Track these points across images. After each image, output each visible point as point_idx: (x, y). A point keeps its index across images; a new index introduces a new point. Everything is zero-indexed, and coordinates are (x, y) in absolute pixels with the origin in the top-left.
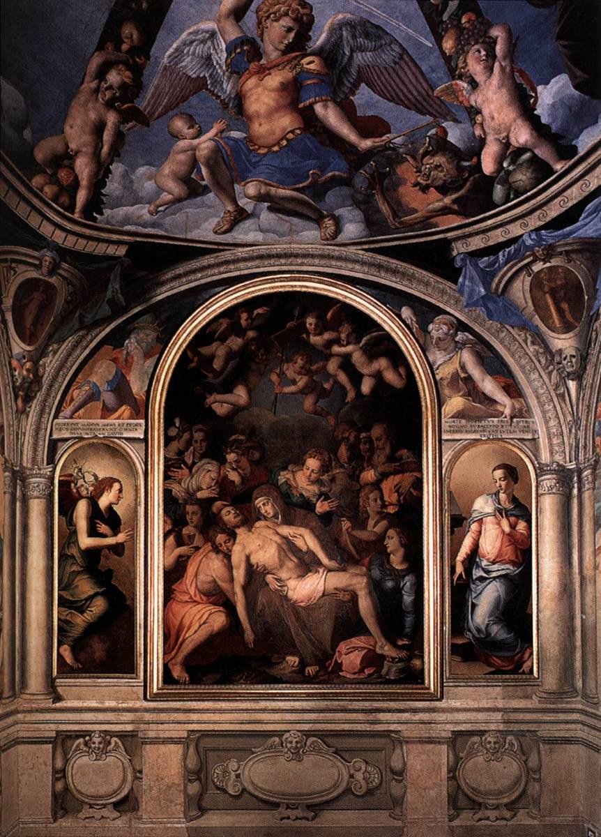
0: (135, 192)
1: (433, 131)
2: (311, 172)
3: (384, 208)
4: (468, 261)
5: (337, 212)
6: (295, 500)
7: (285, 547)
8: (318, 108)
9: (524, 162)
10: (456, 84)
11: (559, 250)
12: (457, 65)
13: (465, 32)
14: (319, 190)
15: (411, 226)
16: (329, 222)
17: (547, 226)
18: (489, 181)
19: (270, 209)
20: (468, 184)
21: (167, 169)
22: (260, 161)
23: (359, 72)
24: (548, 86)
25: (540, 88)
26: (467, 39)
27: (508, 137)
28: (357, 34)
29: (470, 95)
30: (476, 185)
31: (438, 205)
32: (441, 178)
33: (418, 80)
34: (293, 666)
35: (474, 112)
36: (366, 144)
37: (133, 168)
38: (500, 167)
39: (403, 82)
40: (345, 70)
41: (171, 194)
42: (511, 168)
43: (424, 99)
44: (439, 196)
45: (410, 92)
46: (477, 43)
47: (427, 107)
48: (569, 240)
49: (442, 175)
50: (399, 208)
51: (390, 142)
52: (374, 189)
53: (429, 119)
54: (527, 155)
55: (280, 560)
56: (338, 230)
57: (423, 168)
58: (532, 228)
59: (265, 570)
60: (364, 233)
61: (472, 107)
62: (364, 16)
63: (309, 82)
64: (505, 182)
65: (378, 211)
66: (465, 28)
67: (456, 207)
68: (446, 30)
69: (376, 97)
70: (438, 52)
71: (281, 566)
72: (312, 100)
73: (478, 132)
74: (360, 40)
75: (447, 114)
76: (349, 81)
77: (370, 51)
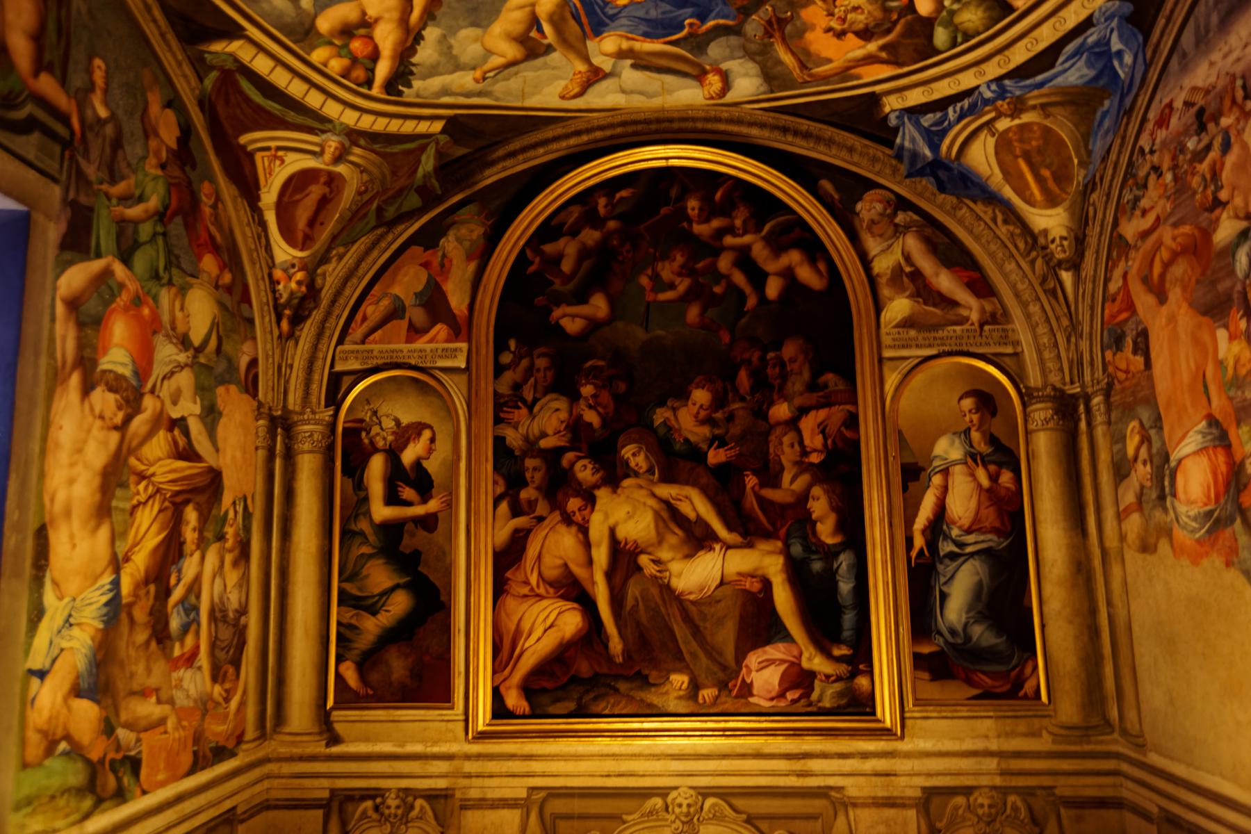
0: (455, 58)
2: (687, 22)
3: (787, 58)
4: (906, 120)
5: (725, 66)
6: (677, 447)
7: (665, 515)
11: (1032, 102)
14: (699, 43)
15: (825, 79)
16: (714, 81)
17: (1009, 75)
18: (928, 24)
19: (634, 66)
20: (899, 28)
21: (498, 28)
22: (620, 12)
30: (909, 32)
31: (859, 53)
32: (861, 22)
34: (680, 689)
37: (453, 31)
41: (502, 56)
42: (955, 7)
44: (860, 42)
48: (1045, 90)
49: (861, 17)
50: (806, 59)
52: (771, 36)
55: (658, 533)
56: (726, 86)
57: (836, 10)
58: (991, 77)
59: (636, 548)
60: (762, 89)
64: (950, 23)
65: (779, 62)
67: (884, 55)
71: (660, 541)
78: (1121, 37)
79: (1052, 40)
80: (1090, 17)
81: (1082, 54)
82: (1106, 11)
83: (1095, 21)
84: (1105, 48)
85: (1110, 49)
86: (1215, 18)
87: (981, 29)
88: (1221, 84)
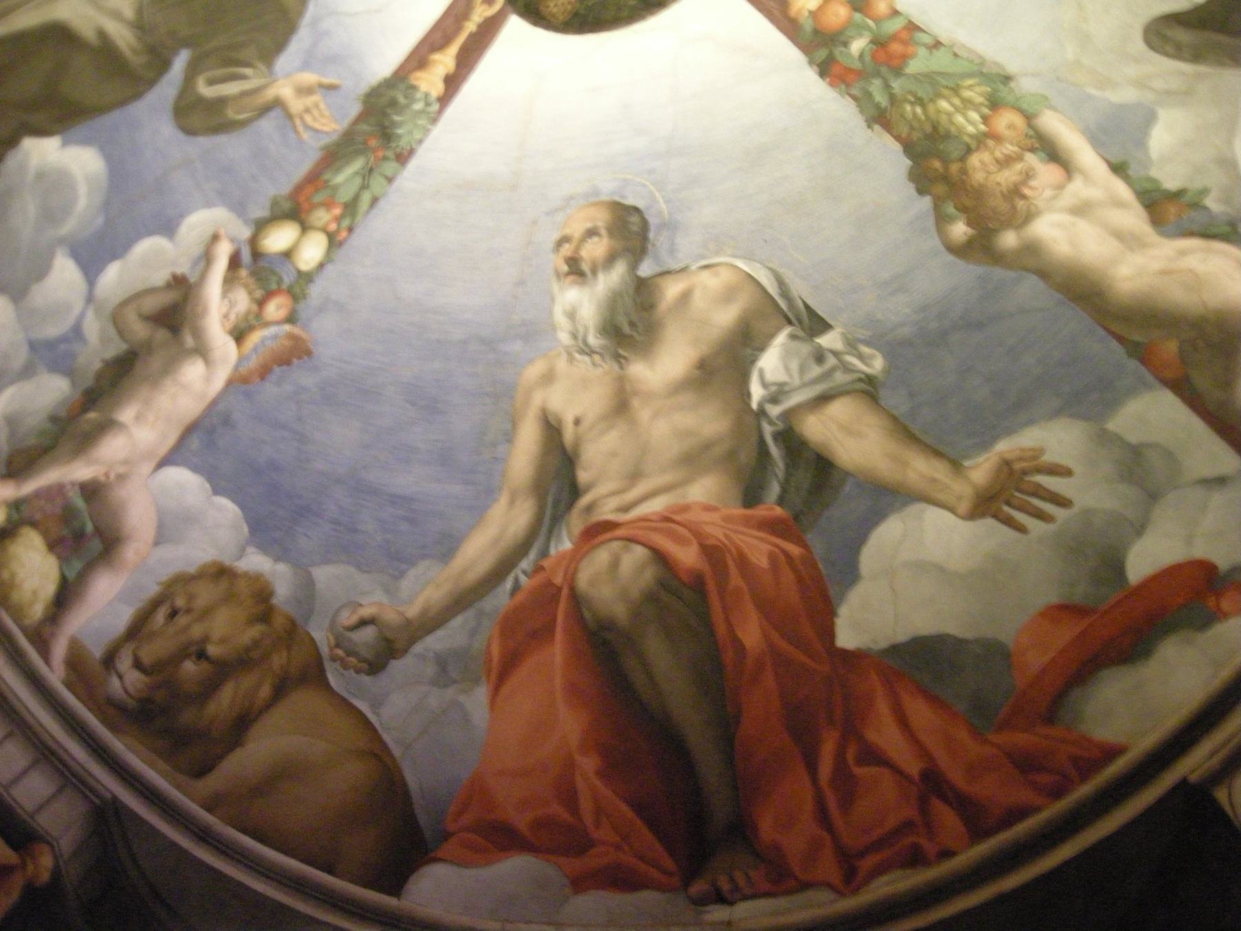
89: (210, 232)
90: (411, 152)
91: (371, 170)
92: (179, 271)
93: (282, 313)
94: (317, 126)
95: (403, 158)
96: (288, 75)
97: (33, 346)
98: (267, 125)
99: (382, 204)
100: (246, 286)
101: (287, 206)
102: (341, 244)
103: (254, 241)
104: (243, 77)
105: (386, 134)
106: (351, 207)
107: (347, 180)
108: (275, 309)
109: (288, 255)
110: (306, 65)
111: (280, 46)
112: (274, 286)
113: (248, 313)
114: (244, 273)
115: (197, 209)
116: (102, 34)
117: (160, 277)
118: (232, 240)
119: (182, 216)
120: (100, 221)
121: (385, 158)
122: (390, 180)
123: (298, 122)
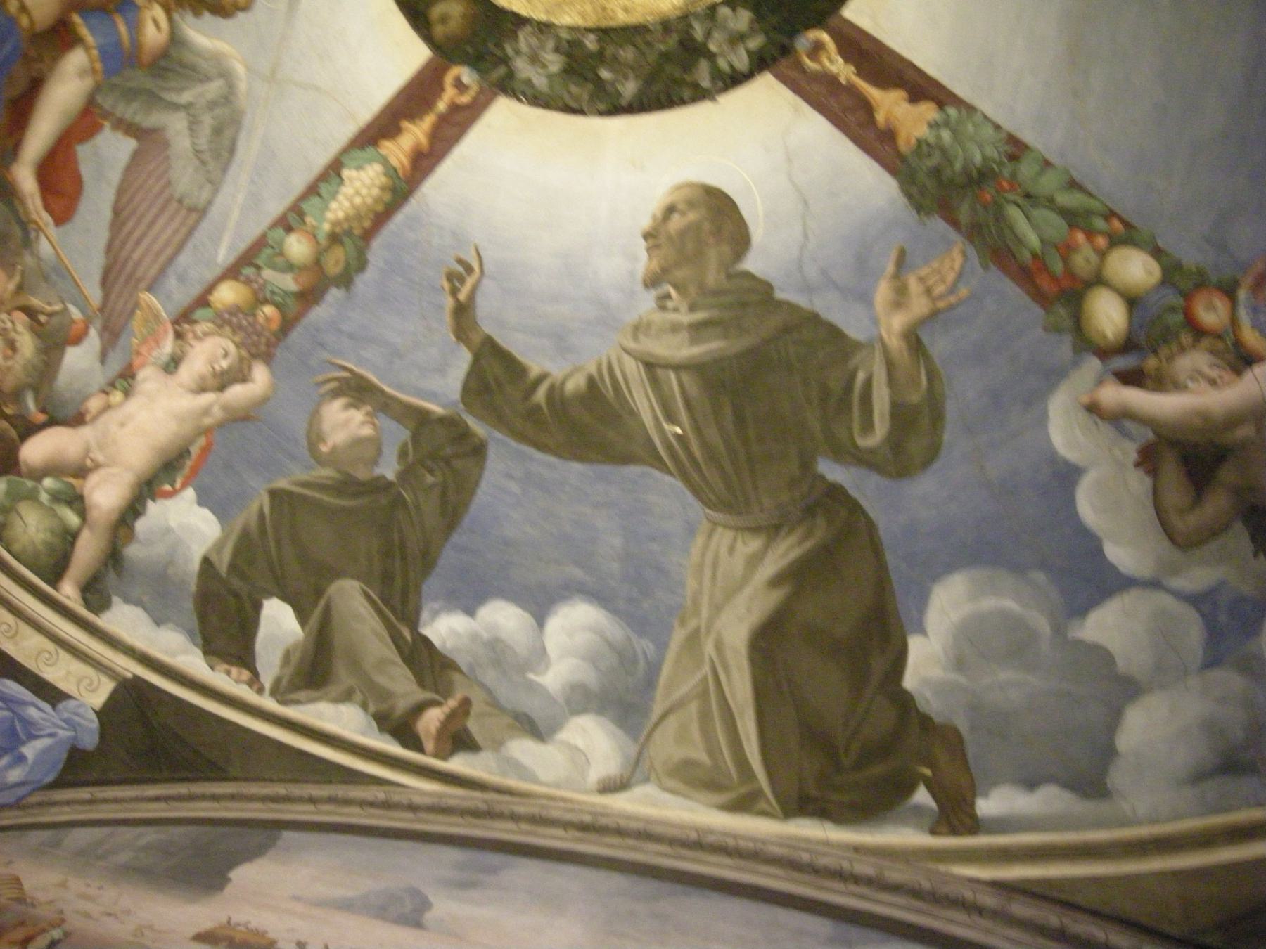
1: (76, 313)
8: (76, 60)
9: (60, 519)
10: (166, 332)
12: (195, 322)
13: (251, 319)
23: (153, 131)
24: (196, 508)
25: (190, 493)
26: (240, 327)
27: (97, 466)
28: (218, 111)
29: (154, 364)
33: (158, 254)
35: (126, 379)
36: (25, 177)
38: (38, 475)
39: (153, 223)
40: (153, 100)
42: (44, 497)
43: (130, 277)
45: (138, 242)
46: (237, 346)
47: (117, 288)
51: (39, 229)
53: (94, 294)
54: (73, 519)
61: (133, 376)
62: (247, 121)
63: (123, 29)
66: (254, 315)
68: (248, 282)
69: (115, 176)
70: (210, 276)
72: (90, 39)
73: (94, 404)
74: (207, 121)
75: (112, 334)
76: (135, 113)
77: (193, 143)
78: (47, 750)
79: (20, 658)
80: (64, 696)
81: (10, 709)
82: (77, 714)
83: (60, 706)
84: (24, 738)
85: (23, 743)
86: (124, 857)
87: (16, 547)
88: (40, 912)
89: (1083, 416)
90: (1013, 140)
91: (1028, 196)
92: (1133, 456)
93: (1221, 304)
94: (951, 277)
95: (1016, 148)
96: (875, 321)
97: (1212, 661)
98: (939, 345)
99: (1076, 175)
100: (1170, 358)
101: (1062, 311)
102: (1126, 224)
103: (1104, 353)
104: (868, 383)
105: (980, 177)
106: (1073, 218)
107: (1034, 226)
108: (1212, 313)
109: (1132, 302)
110: (866, 299)
111: (835, 333)
112: (1179, 318)
113: (1212, 352)
114: (1151, 363)
115: (1048, 440)
116: (775, 582)
117: (1139, 483)
118: (1100, 382)
119: (1053, 458)
120: (1040, 577)
121: (1014, 175)
122: (1047, 164)
123: (941, 305)
